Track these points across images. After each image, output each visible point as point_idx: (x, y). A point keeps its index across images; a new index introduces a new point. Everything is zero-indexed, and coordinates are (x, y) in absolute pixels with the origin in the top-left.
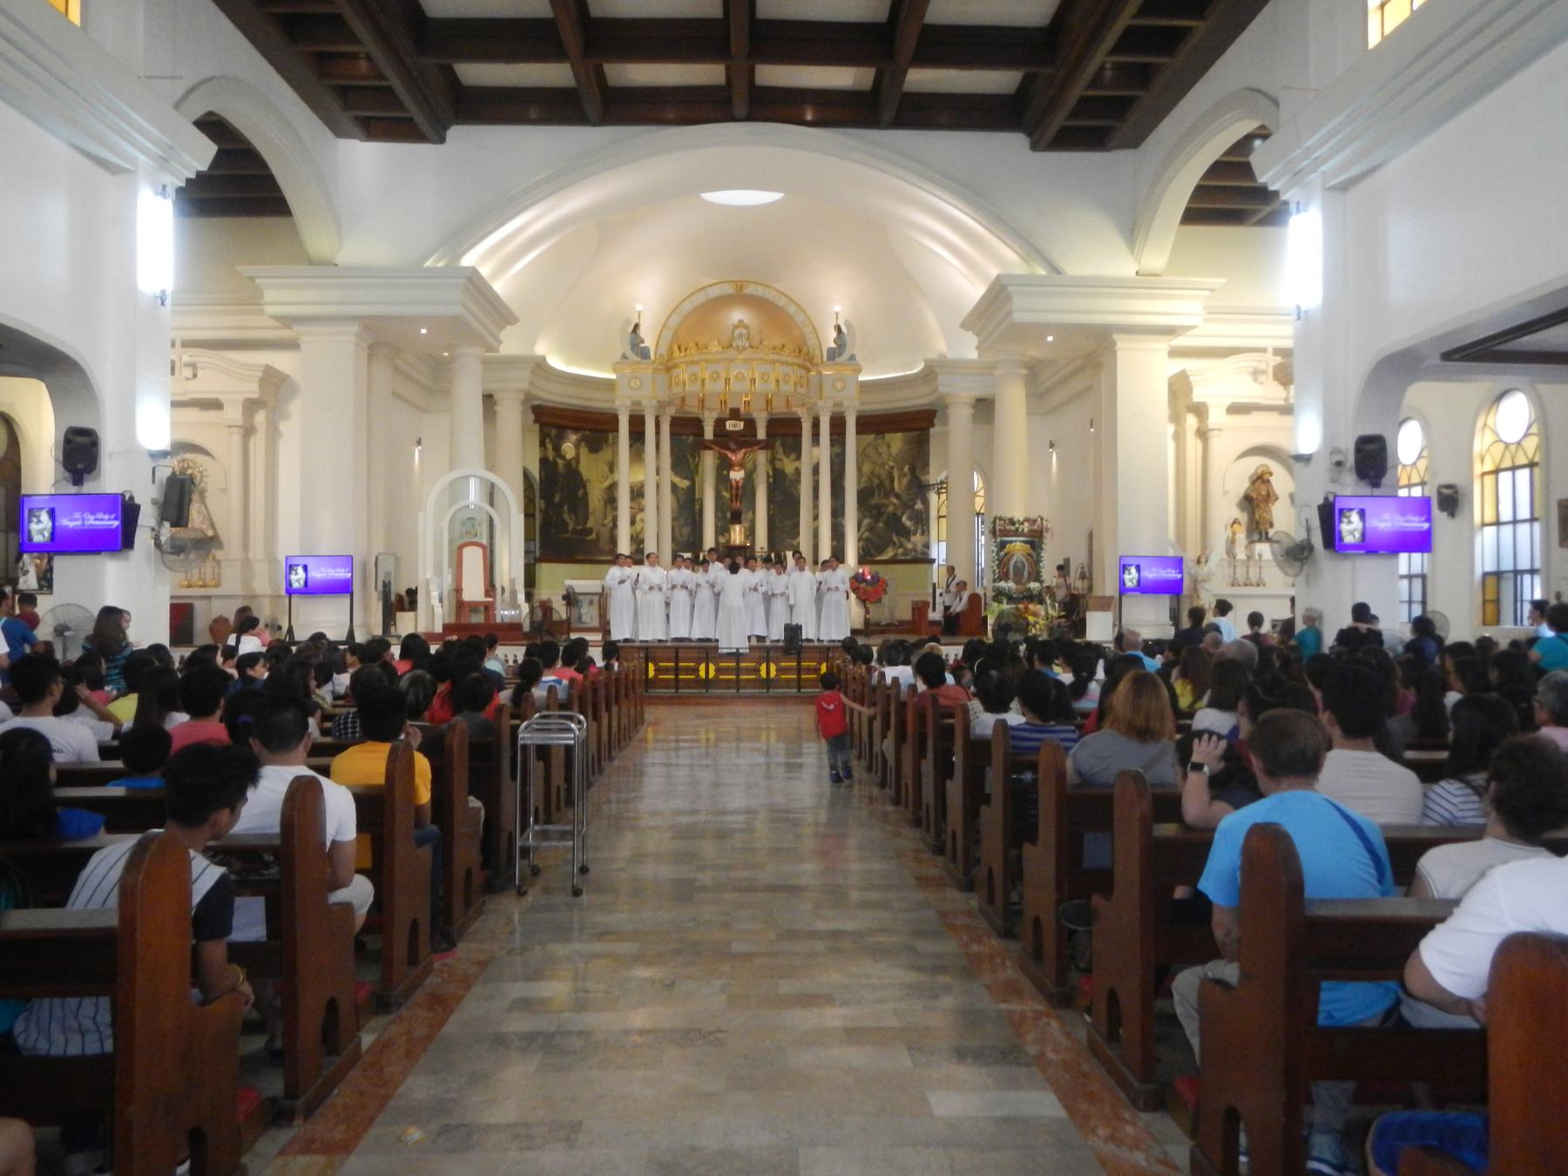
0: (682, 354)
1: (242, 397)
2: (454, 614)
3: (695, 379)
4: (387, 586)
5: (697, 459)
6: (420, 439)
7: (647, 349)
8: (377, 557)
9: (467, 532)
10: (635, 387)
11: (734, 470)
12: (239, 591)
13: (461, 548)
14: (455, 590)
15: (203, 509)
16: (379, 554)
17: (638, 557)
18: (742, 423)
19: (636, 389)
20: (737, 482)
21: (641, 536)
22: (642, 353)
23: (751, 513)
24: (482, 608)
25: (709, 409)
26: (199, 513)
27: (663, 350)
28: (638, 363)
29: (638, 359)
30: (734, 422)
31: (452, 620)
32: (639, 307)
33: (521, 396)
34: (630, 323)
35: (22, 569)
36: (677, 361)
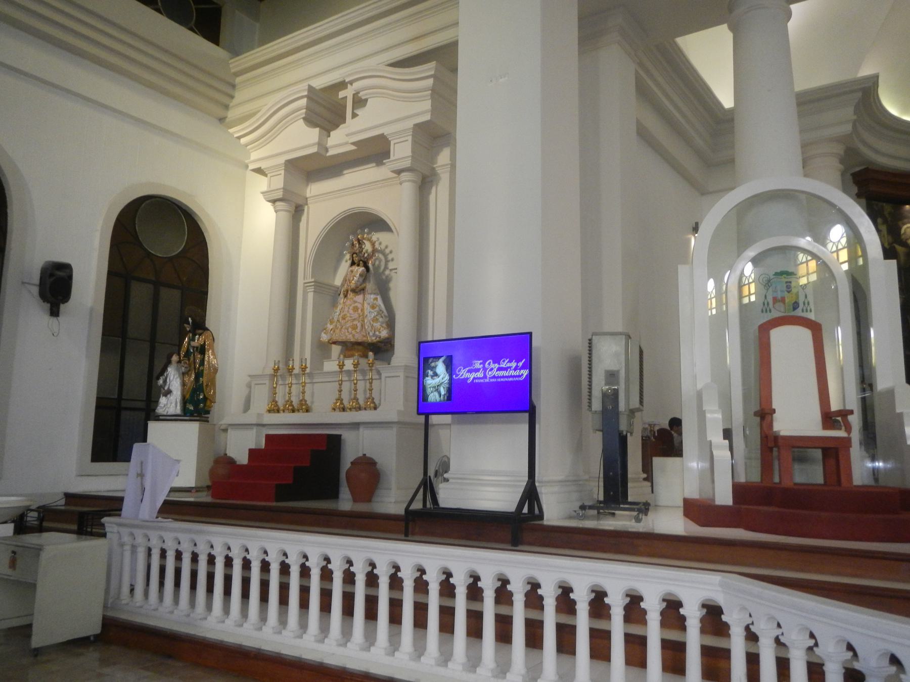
1: (410, 124)
2: (756, 465)
4: (611, 398)
6: (697, 224)
8: (590, 340)
9: (775, 300)
12: (394, 417)
13: (765, 329)
14: (756, 414)
15: (380, 301)
16: (594, 334)
24: (818, 454)
26: (373, 307)
31: (751, 475)
33: (839, 149)
35: (162, 387)
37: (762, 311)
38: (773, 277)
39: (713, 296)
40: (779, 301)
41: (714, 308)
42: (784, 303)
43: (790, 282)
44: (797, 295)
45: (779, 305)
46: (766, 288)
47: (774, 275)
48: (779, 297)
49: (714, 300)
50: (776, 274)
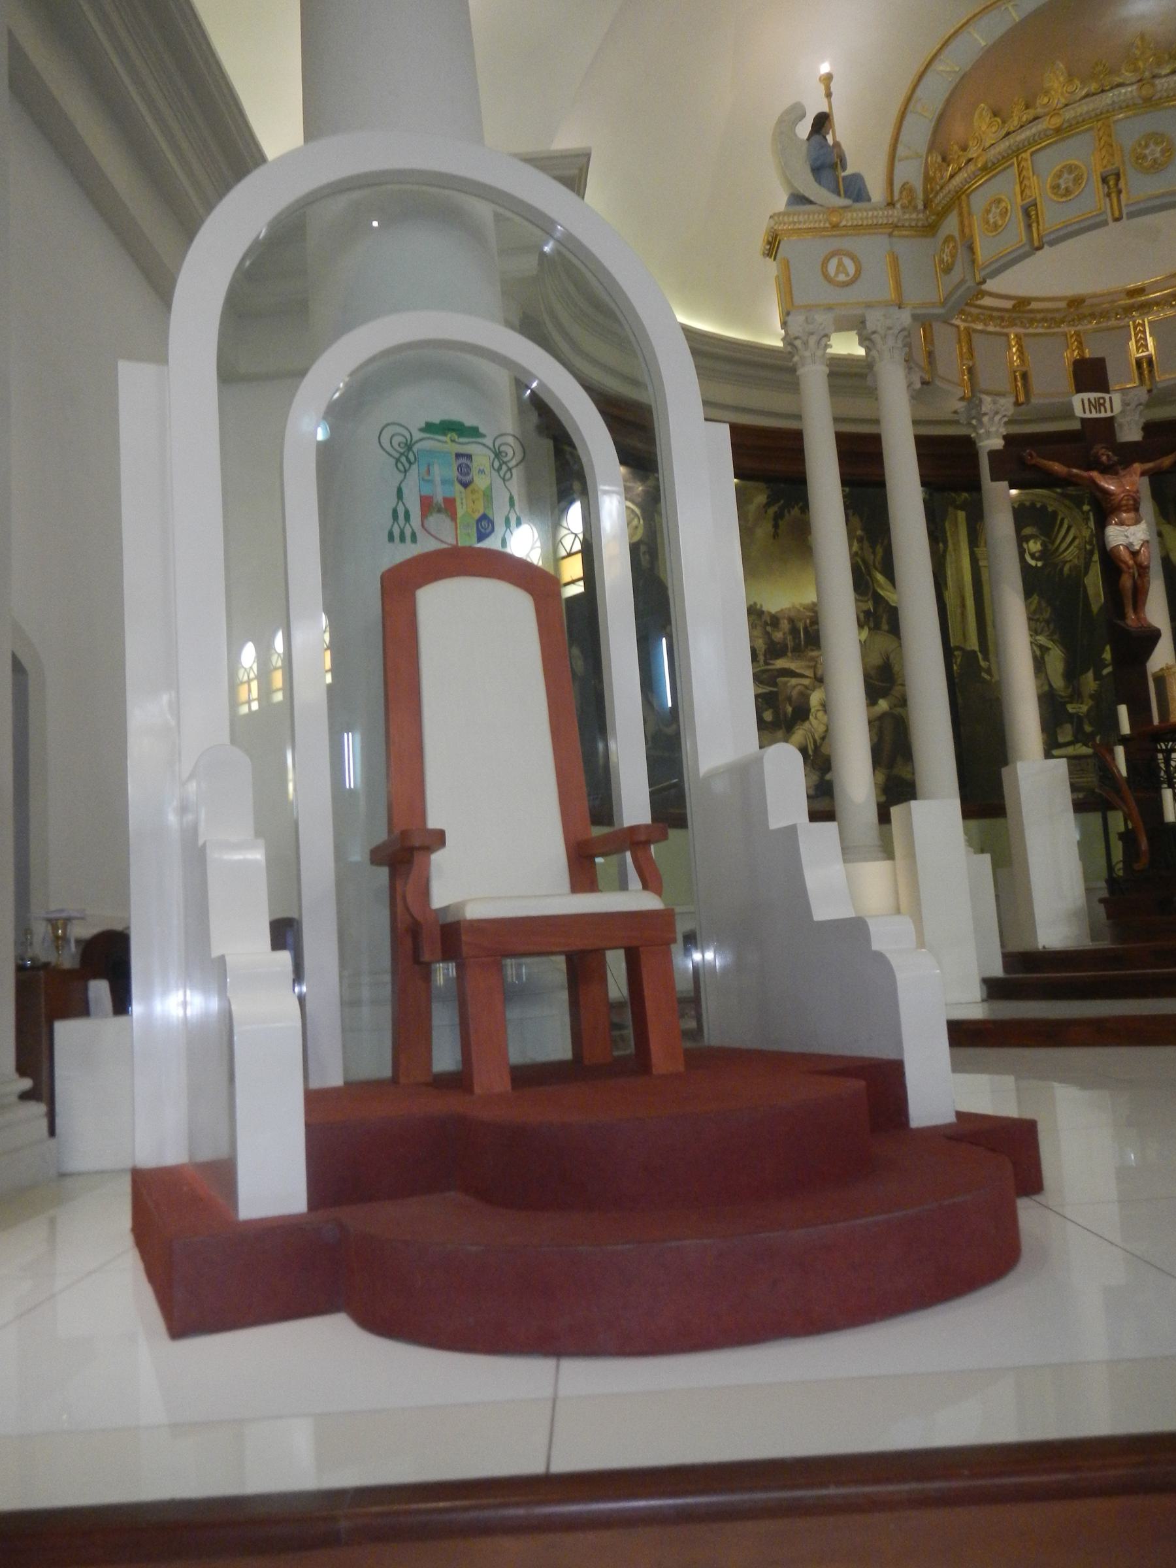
0: (1014, 123)
3: (1077, 180)
5: (941, 545)
7: (857, 178)
9: (427, 505)
10: (842, 278)
11: (1121, 523)
14: (377, 856)
17: (822, 805)
18: (1117, 398)
19: (846, 284)
20: (1135, 554)
21: (824, 750)
22: (846, 192)
23: (1090, 675)
25: (988, 393)
27: (910, 173)
28: (845, 208)
29: (843, 202)
30: (1093, 396)
32: (825, 68)
34: (803, 116)
36: (992, 154)
37: (391, 537)
38: (417, 435)
39: (252, 675)
40: (439, 511)
41: (254, 700)
42: (453, 517)
43: (469, 457)
44: (488, 496)
45: (438, 522)
46: (400, 465)
47: (421, 430)
48: (439, 498)
49: (254, 685)
50: (429, 428)
